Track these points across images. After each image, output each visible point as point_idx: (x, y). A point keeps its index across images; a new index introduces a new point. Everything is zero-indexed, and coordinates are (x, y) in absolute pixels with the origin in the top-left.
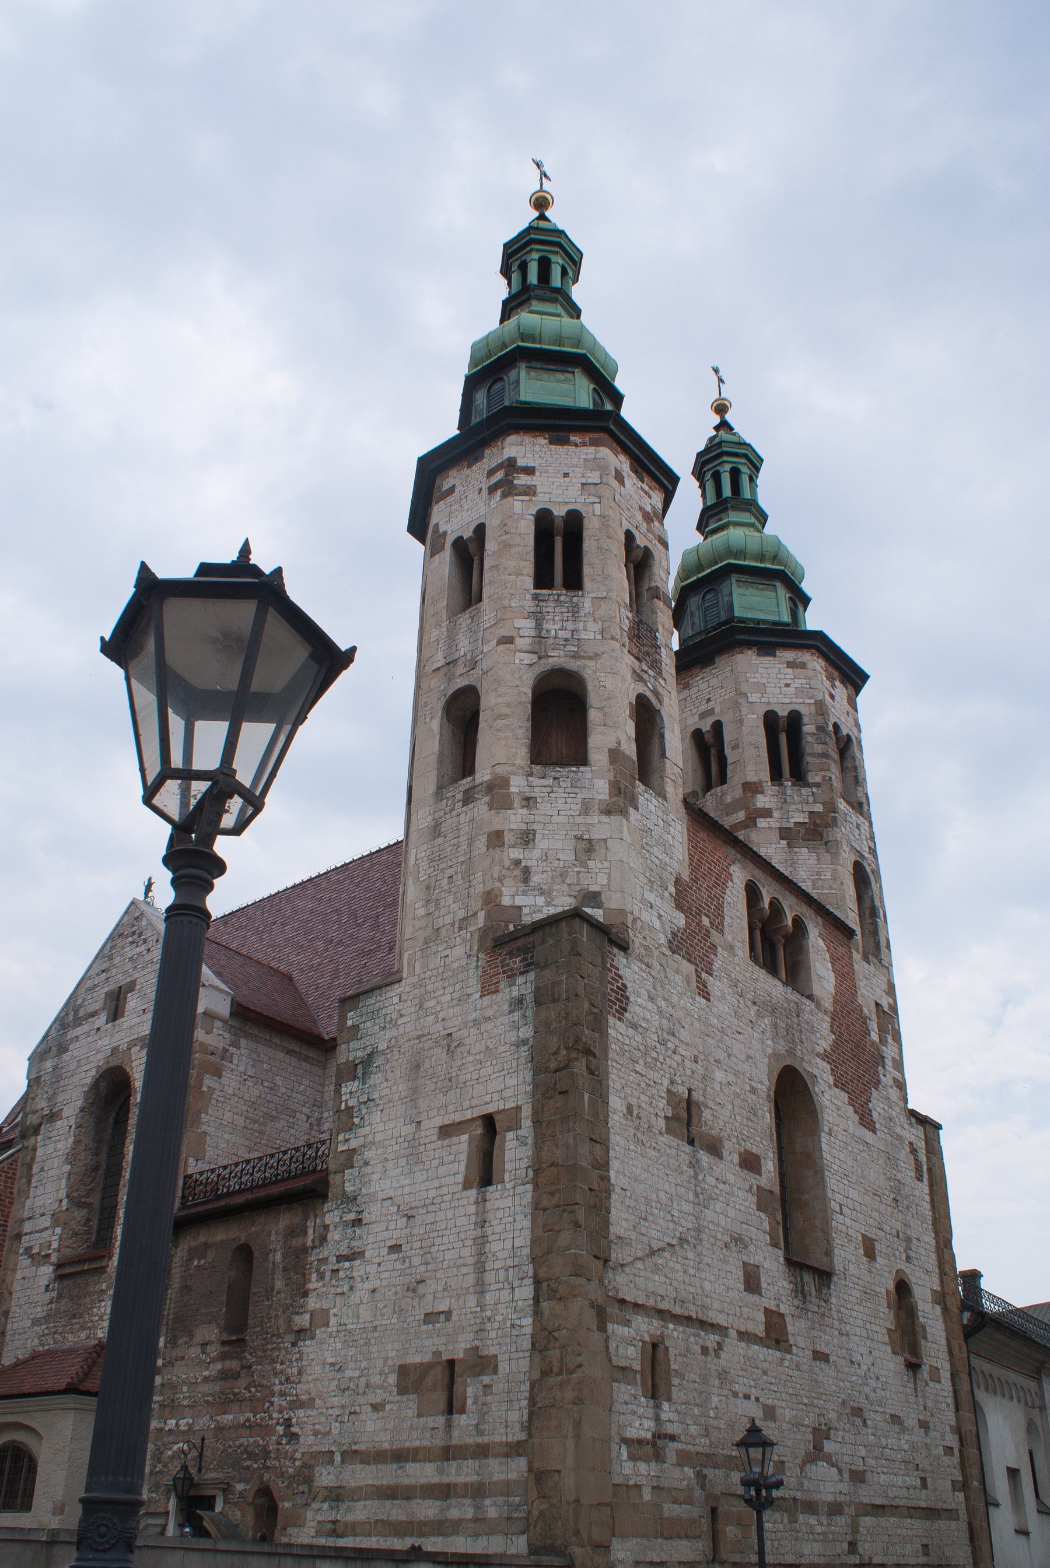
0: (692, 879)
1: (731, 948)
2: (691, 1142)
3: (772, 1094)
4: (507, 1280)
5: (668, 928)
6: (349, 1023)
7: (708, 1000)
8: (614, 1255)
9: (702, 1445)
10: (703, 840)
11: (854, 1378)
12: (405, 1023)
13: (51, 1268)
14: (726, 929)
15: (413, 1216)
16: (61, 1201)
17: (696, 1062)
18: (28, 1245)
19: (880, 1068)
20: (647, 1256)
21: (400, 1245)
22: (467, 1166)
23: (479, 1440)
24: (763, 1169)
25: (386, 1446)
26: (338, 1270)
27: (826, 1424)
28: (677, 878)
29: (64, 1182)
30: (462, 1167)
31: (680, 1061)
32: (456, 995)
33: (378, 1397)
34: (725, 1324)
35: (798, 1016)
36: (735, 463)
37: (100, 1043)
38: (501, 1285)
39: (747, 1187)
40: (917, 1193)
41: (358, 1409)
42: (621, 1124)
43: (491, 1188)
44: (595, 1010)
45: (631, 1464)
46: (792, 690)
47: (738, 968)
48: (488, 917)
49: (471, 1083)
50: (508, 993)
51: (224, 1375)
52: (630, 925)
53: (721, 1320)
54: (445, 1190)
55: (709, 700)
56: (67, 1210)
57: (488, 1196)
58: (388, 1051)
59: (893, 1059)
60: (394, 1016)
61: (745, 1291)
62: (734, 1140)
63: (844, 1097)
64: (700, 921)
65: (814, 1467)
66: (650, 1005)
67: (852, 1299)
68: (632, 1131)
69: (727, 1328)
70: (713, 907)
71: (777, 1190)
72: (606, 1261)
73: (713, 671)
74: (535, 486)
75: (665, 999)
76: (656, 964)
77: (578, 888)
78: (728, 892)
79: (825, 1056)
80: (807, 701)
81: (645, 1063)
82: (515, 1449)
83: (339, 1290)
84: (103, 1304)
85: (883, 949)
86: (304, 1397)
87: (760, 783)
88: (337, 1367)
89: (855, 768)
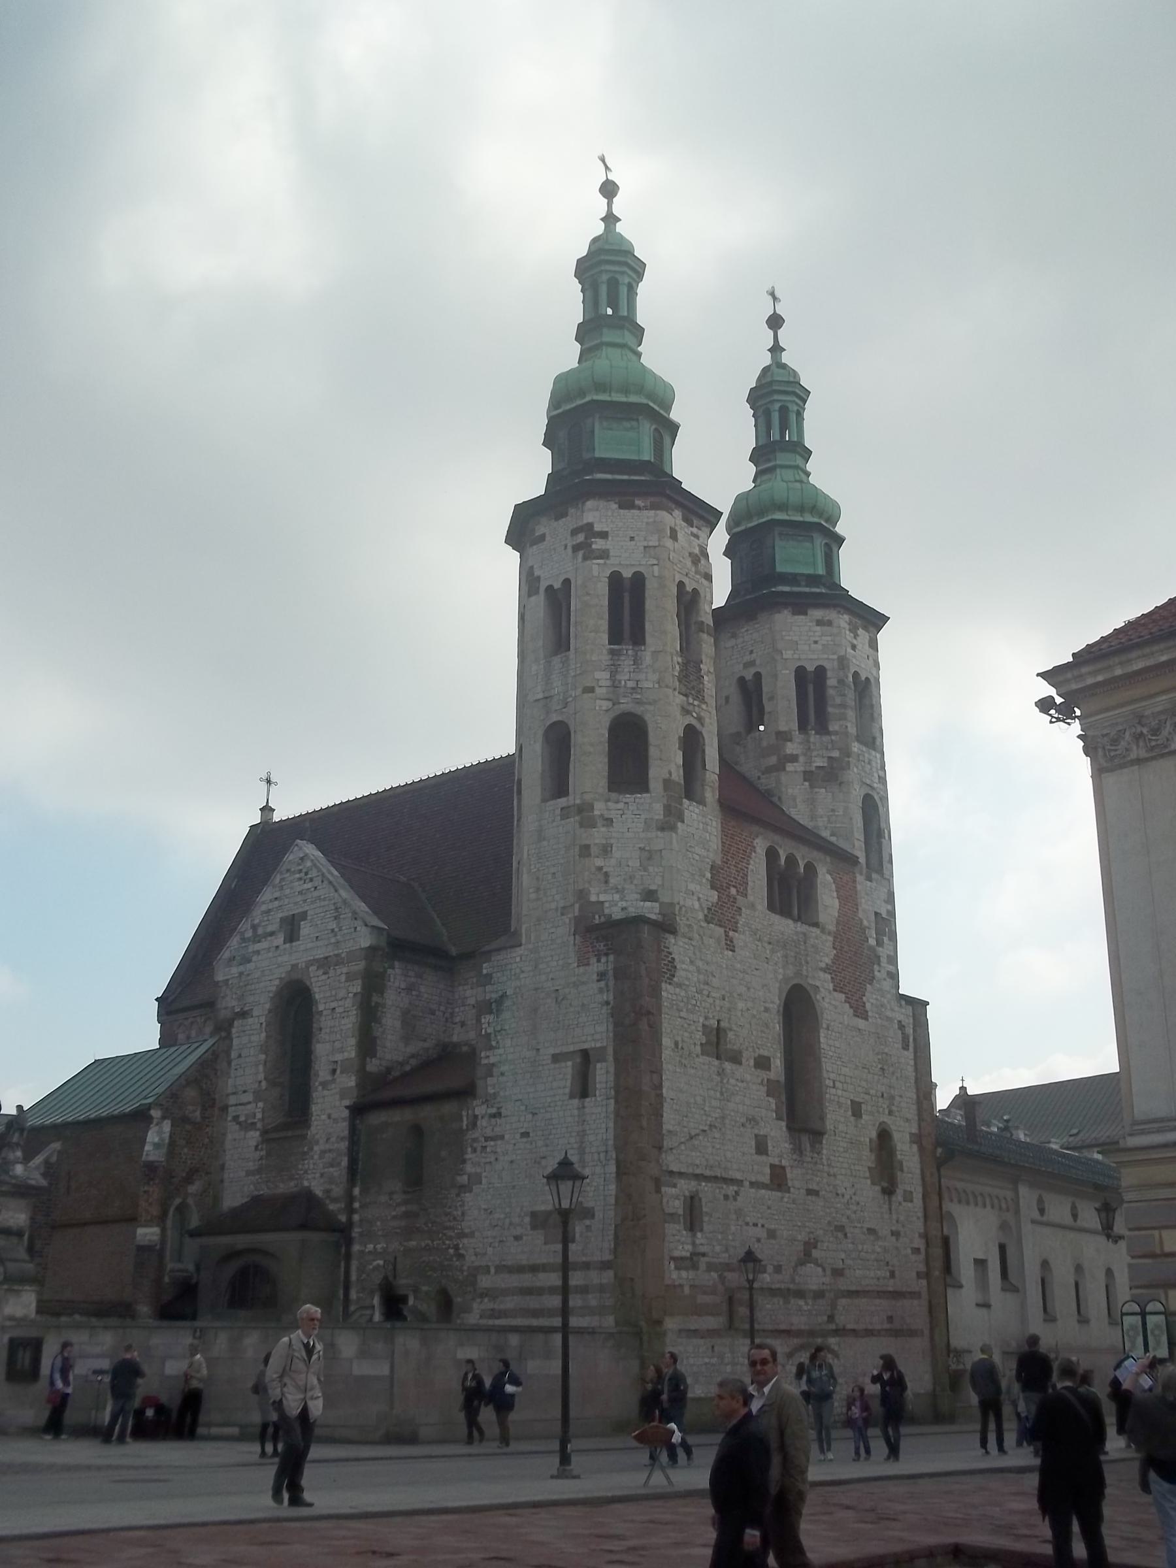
0: (724, 862)
1: (752, 906)
2: (717, 1059)
3: (781, 1009)
4: (599, 1160)
5: (704, 906)
6: (485, 972)
7: (733, 951)
8: (665, 1143)
9: (724, 1258)
10: (734, 827)
11: (839, 1205)
12: (525, 978)
13: (258, 1133)
14: (749, 891)
15: (536, 1114)
16: (260, 1082)
17: (724, 999)
18: (234, 1114)
19: (875, 966)
20: (687, 1140)
21: (528, 1133)
22: (572, 1084)
23: (584, 1259)
24: (772, 1066)
25: (524, 1262)
26: (486, 1147)
27: (814, 1239)
28: (712, 866)
29: (261, 1068)
30: (569, 1083)
31: (712, 1002)
32: (561, 962)
33: (519, 1231)
34: (742, 1179)
35: (805, 943)
36: (785, 401)
37: (280, 959)
38: (595, 1163)
39: (760, 1081)
40: (903, 1060)
41: (504, 1239)
42: (670, 1056)
43: (588, 1100)
44: (653, 983)
45: (677, 1272)
46: (819, 647)
47: (757, 920)
48: (580, 910)
49: (571, 1027)
50: (595, 967)
51: (407, 1215)
52: (677, 913)
53: (738, 1176)
54: (557, 1098)
55: (751, 652)
56: (266, 1089)
57: (586, 1104)
58: (514, 996)
59: (888, 956)
60: (518, 971)
61: (756, 1153)
62: (751, 1050)
63: (842, 997)
64: (729, 893)
65: (803, 1267)
66: (692, 968)
67: (839, 1149)
68: (678, 1059)
69: (742, 1181)
70: (739, 878)
71: (782, 1079)
72: (660, 1148)
73: (756, 626)
74: (608, 550)
75: (702, 960)
76: (696, 936)
77: (641, 887)
78: (752, 862)
79: (825, 970)
80: (831, 657)
81: (687, 1010)
82: (605, 1266)
83: (488, 1160)
84: (306, 1162)
85: (885, 864)
86: (467, 1231)
87: (790, 732)
88: (489, 1211)
89: (872, 706)
